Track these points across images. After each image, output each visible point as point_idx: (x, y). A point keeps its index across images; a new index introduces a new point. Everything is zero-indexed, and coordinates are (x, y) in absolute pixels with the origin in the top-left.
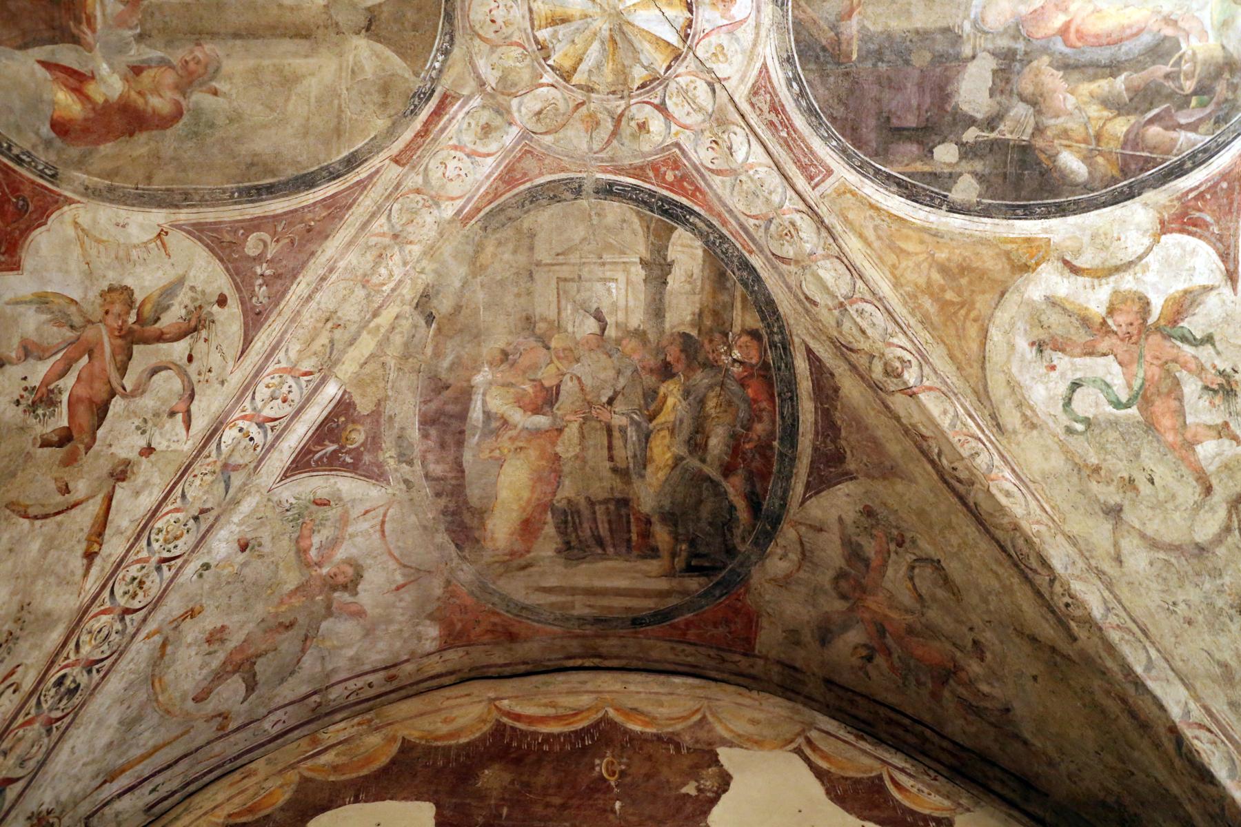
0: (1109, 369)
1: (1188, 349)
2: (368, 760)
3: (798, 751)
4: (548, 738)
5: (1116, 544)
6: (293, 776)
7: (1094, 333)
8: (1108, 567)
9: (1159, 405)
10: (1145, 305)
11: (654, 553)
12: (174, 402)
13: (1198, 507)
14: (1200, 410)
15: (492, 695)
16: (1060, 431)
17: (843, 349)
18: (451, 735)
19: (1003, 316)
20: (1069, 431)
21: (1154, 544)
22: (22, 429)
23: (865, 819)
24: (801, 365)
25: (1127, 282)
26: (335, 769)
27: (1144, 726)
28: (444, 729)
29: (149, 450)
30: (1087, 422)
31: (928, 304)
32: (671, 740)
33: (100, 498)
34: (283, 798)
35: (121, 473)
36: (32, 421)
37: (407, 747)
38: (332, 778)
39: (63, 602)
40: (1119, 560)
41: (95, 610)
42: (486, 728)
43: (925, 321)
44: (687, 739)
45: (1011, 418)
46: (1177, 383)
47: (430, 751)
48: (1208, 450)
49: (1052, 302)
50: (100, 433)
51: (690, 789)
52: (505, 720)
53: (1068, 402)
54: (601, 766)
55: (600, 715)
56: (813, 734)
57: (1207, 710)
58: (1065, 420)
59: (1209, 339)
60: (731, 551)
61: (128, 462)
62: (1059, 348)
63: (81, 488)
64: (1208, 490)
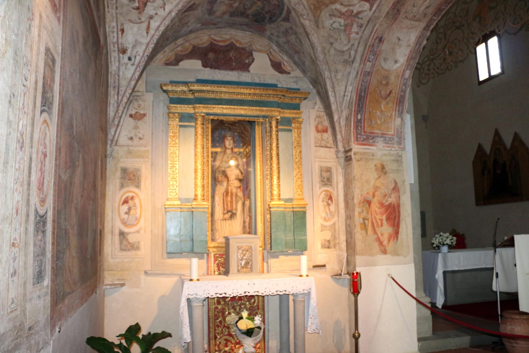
0: (342, 21)
1: (357, 19)
2: (187, 50)
3: (268, 54)
4: (221, 46)
5: (330, 49)
6: (173, 53)
7: (342, 15)
8: (326, 52)
9: (348, 27)
10: (353, 11)
11: (248, 18)
12: (161, 5)
13: (346, 45)
14: (355, 28)
15: (209, 33)
16: (328, 29)
17: (294, 9)
18: (203, 44)
19: (325, 10)
20: (330, 29)
21: (336, 50)
22: (128, 5)
23: (276, 71)
24: (286, 8)
25: (351, 8)
26: (181, 51)
27: (322, 76)
28: (201, 42)
29: (156, 14)
30: (334, 28)
31: (312, 7)
32: (244, 49)
33: (147, 22)
34: (173, 57)
35: (151, 18)
36: (130, 4)
37: (194, 47)
38: (181, 53)
39: (145, 41)
40: (329, 52)
41: (150, 43)
42: (209, 43)
43: (311, 9)
44: (247, 49)
45: (320, 26)
46: (353, 24)
47: (199, 48)
48: (353, 35)
49: (336, 9)
50: (146, 8)
51: (247, 61)
52: (213, 41)
53: (332, 25)
54: (231, 54)
55: (231, 41)
56: (271, 50)
57: (331, 77)
58: (330, 27)
59: (362, 18)
60: (264, 21)
61: (152, 16)
62: (334, 16)
63: (143, 19)
64: (349, 42)
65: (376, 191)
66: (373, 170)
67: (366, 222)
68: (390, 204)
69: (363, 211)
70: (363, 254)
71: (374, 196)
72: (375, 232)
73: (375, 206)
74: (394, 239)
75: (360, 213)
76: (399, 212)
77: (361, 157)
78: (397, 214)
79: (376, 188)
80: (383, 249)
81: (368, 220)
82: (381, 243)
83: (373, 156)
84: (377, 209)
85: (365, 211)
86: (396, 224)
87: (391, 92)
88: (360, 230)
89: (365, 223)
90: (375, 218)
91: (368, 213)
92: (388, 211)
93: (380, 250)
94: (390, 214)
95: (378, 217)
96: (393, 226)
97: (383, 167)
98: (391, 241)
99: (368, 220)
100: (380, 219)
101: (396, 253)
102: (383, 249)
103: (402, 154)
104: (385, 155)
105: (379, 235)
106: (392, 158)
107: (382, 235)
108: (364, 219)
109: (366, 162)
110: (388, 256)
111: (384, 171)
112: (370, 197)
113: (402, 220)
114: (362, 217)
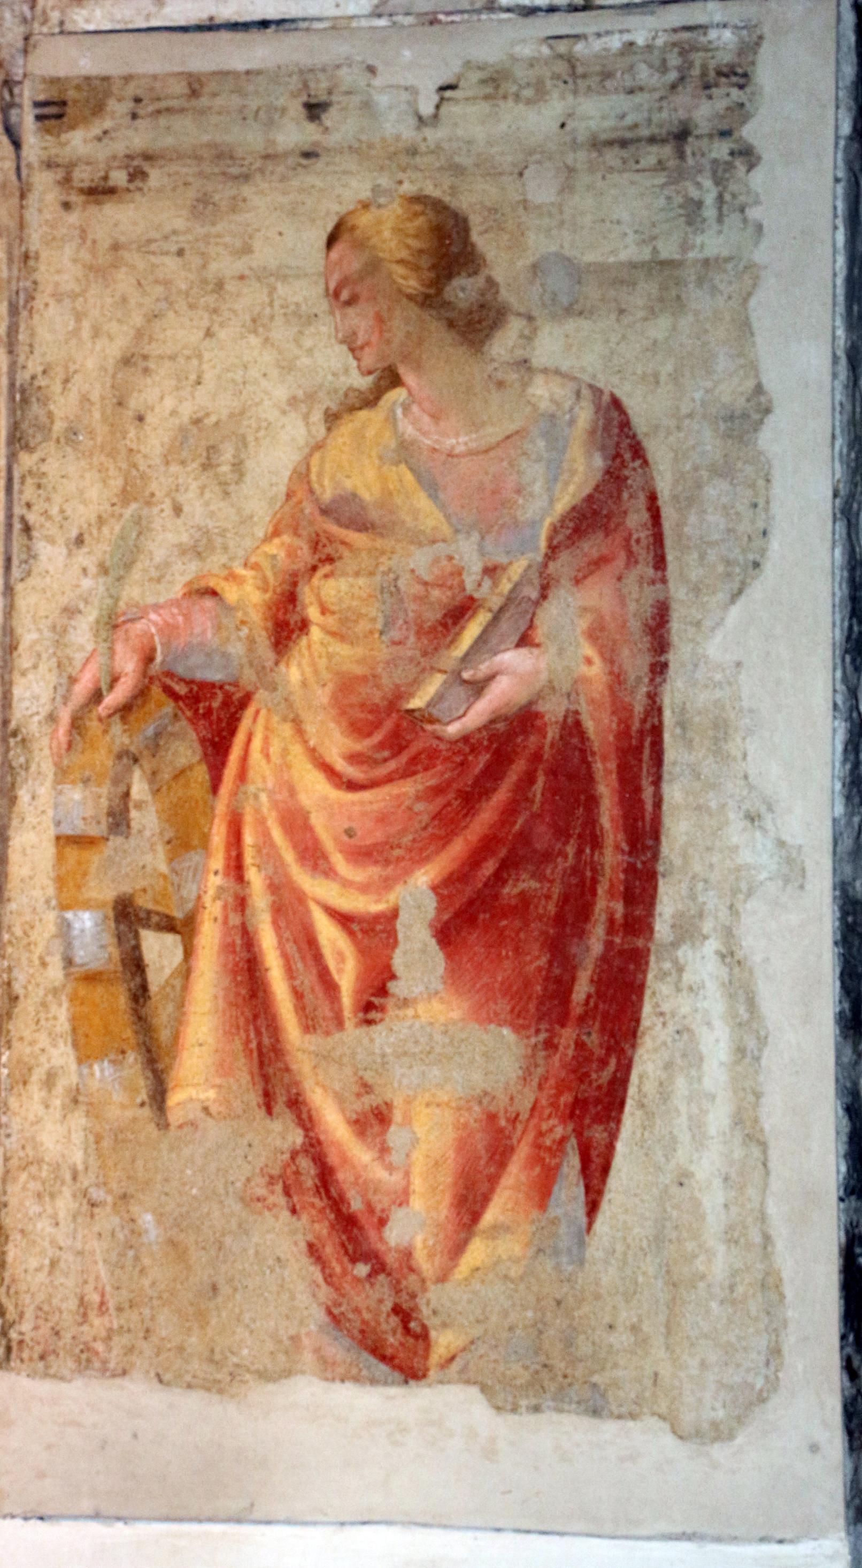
65: (324, 556)
66: (308, 293)
67: (160, 950)
68: (525, 719)
69: (119, 819)
70: (87, 1360)
71: (286, 627)
72: (273, 1083)
73: (293, 759)
74: (543, 1191)
75: (68, 842)
76: (643, 833)
77: (138, 138)
78: (611, 859)
79: (326, 528)
80: (373, 1300)
81: (183, 927)
82: (349, 1232)
83: (314, 110)
84: (314, 789)
85: (147, 820)
86: (582, 989)
88: (62, 1055)
89: (135, 964)
90: (289, 905)
91: (183, 840)
92: (486, 815)
93: (336, 1319)
94: (513, 849)
96: (544, 1006)
97: (448, 245)
98: (490, 1216)
99: (183, 927)
100: (344, 920)
101: (554, 1371)
102: (373, 1300)
103: (751, 46)
104: (496, 83)
105: (334, 1123)
106: (598, 112)
107: (374, 1121)
108: (127, 916)
109: (203, 206)
111: (463, 290)
112: (224, 647)
113: (688, 930)
114: (105, 890)
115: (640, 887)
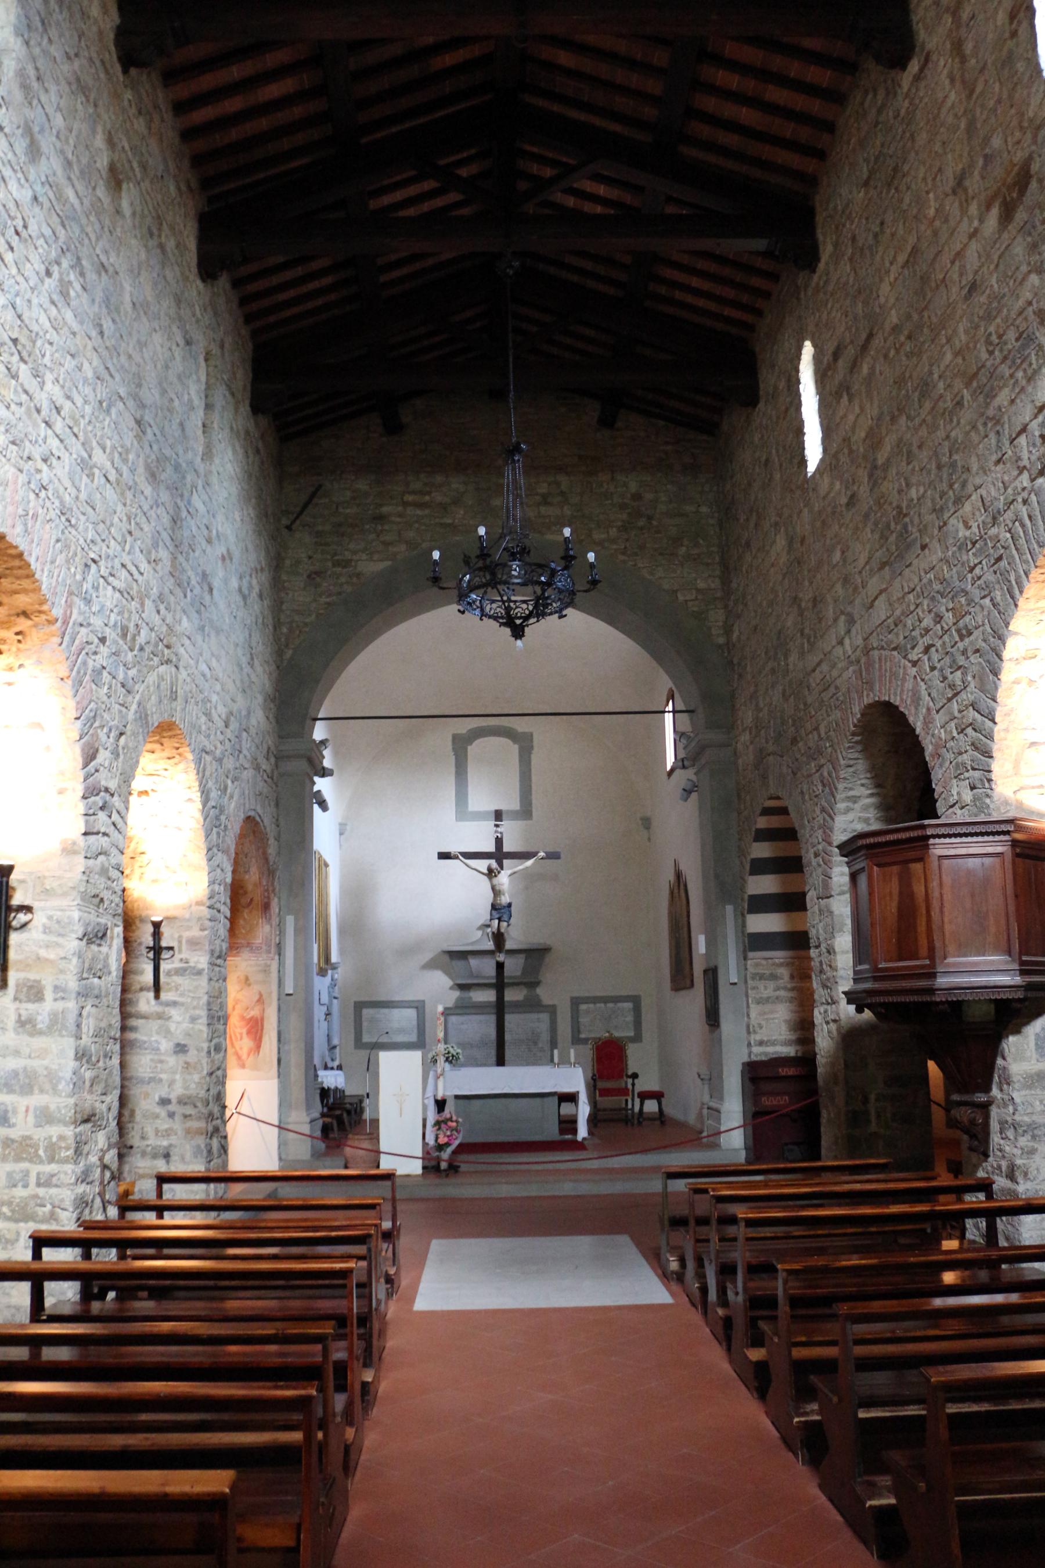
76: (262, 1026)
82: (239, 1058)
87: (252, 900)
94: (252, 1027)
95: (238, 1030)
96: (255, 1039)
97: (247, 979)
101: (255, 1068)
105: (238, 1048)
107: (241, 1048)
110: (246, 1071)
115: (262, 1030)
